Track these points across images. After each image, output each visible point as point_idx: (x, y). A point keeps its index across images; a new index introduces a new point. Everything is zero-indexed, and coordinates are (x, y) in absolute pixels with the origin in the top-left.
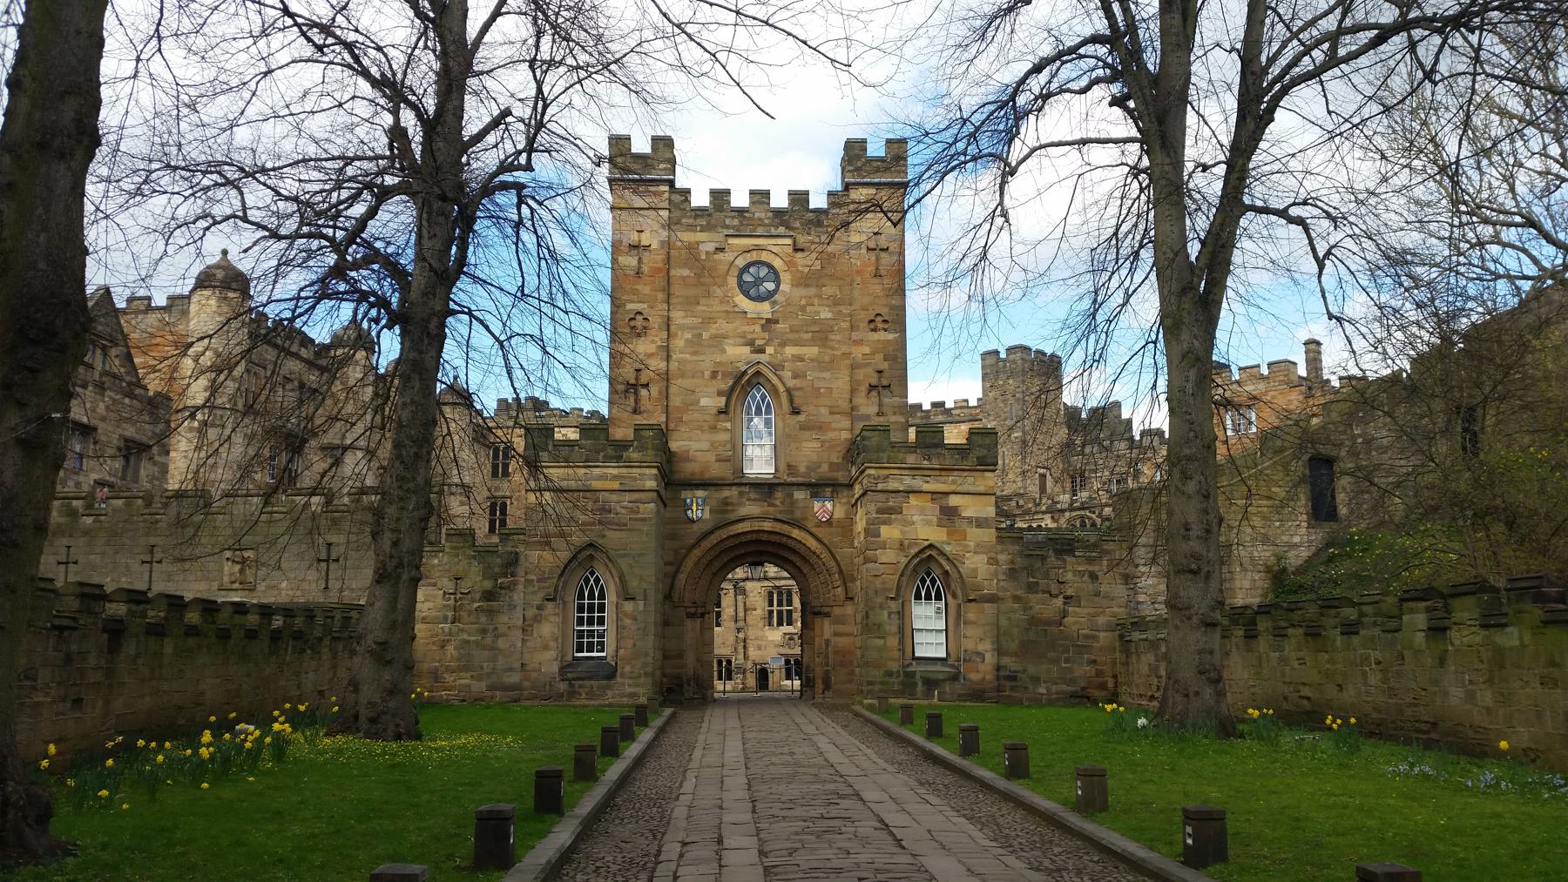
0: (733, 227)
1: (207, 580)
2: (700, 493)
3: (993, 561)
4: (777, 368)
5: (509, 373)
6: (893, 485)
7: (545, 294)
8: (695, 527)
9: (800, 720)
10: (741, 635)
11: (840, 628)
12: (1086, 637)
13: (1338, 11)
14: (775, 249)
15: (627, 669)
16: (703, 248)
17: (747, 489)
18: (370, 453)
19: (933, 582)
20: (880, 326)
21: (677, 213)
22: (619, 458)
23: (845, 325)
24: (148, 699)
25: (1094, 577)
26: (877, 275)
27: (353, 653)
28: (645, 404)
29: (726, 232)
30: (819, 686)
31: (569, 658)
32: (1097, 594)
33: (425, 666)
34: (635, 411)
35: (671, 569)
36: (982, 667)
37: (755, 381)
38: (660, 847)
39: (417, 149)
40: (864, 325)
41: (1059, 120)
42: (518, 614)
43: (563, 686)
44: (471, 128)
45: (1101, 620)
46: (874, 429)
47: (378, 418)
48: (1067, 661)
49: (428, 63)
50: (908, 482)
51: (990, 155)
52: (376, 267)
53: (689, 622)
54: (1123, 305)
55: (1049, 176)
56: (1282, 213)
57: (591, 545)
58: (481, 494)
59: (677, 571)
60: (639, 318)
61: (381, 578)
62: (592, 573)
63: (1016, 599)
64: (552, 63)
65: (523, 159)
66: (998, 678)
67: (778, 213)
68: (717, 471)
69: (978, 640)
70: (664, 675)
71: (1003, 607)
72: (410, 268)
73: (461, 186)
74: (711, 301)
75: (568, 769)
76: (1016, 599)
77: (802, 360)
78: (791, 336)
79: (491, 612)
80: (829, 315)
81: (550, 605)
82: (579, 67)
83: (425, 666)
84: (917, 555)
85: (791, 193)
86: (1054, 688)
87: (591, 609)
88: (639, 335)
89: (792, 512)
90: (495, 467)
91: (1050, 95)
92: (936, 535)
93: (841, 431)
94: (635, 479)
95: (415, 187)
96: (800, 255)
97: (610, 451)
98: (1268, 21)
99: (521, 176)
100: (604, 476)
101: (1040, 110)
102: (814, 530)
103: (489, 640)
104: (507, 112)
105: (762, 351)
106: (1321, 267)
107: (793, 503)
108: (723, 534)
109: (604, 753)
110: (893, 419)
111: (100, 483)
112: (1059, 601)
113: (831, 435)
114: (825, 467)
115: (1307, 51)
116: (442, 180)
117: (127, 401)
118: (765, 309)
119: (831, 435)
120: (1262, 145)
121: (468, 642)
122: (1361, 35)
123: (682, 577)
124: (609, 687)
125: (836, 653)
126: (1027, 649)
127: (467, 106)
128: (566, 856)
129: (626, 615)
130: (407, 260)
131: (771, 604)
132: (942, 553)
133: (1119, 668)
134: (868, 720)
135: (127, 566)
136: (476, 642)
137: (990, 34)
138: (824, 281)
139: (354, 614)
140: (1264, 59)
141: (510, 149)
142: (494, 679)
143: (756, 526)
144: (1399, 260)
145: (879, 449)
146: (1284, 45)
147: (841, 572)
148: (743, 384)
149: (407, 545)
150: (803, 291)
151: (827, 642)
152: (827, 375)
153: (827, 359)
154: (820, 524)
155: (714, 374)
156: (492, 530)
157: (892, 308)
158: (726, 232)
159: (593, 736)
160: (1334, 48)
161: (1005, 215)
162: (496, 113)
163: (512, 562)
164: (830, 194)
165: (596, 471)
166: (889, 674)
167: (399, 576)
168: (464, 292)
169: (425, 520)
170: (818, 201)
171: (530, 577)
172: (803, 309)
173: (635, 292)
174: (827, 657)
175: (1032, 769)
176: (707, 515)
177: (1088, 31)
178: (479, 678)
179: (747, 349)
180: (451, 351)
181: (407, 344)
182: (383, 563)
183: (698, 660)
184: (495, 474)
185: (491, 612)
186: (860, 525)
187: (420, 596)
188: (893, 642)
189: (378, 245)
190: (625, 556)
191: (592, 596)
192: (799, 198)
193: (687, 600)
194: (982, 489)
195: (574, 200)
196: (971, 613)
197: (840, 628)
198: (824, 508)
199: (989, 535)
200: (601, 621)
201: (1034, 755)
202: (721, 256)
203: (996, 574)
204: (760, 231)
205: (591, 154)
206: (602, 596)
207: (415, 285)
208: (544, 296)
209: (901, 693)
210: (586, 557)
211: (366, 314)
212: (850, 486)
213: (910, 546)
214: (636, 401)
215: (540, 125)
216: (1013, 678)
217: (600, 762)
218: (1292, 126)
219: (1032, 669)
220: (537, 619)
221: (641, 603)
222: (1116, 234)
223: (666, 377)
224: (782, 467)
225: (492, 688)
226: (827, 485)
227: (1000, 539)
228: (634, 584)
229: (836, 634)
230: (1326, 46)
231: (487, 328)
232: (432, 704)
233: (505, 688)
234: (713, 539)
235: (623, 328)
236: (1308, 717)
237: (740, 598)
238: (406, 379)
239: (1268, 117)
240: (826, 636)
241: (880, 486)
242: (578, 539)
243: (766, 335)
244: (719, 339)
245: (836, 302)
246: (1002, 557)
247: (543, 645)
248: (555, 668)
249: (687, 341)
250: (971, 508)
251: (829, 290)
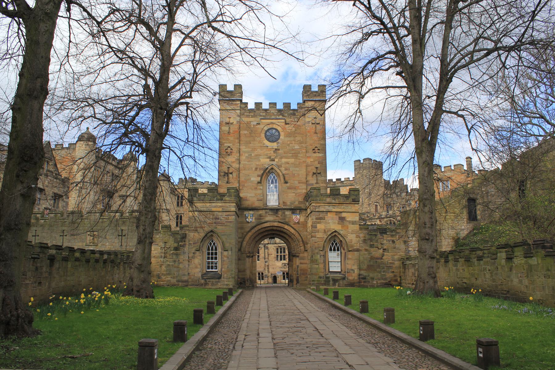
0: (263, 116)
1: (81, 242)
2: (251, 212)
3: (358, 237)
4: (279, 166)
5: (183, 169)
6: (322, 209)
7: (195, 140)
8: (249, 225)
9: (288, 294)
10: (267, 264)
11: (302, 261)
12: (391, 263)
13: (473, 44)
14: (278, 124)
15: (225, 275)
16: (252, 123)
17: (268, 211)
18: (136, 198)
19: (336, 244)
20: (317, 151)
21: (243, 111)
22: (222, 200)
23: (304, 151)
24: (63, 283)
25: (393, 242)
26: (316, 133)
27: (131, 268)
28: (231, 180)
29: (261, 118)
30: (295, 282)
31: (205, 271)
32: (395, 248)
33: (155, 273)
34: (227, 183)
35: (240, 240)
36: (353, 275)
37: (271, 171)
38: (237, 336)
39: (153, 92)
40: (311, 151)
41: (379, 79)
42: (186, 255)
43: (203, 281)
44: (171, 84)
45: (396, 257)
46: (315, 189)
47: (138, 185)
48: (384, 272)
49: (157, 62)
50: (327, 208)
51: (355, 91)
52: (138, 133)
53: (247, 259)
54: (403, 145)
55: (376, 99)
56: (456, 113)
57: (212, 231)
58: (173, 213)
59: (243, 241)
60: (229, 149)
61: (140, 242)
62: (212, 241)
63: (366, 250)
64: (200, 61)
65: (189, 94)
66: (359, 278)
67: (280, 111)
68: (257, 204)
69: (352, 265)
70: (238, 278)
71: (362, 253)
72: (149, 133)
73: (167, 104)
75: (205, 310)
76: (366, 250)
77: (288, 164)
79: (177, 255)
80: (298, 147)
81: (198, 252)
82: (208, 62)
83: (155, 273)
84: (330, 234)
85: (284, 104)
86: (379, 282)
87: (212, 254)
88: (229, 155)
89: (285, 219)
90: (178, 203)
91: (375, 71)
92: (338, 228)
93: (303, 190)
94: (227, 207)
95: (152, 105)
96: (287, 126)
97: (219, 197)
98: (449, 47)
99: (188, 100)
100: (216, 206)
101: (372, 76)
102: (293, 226)
103: (176, 264)
104: (184, 78)
105: (274, 160)
106: (470, 132)
107: (285, 216)
108: (260, 227)
109: (218, 305)
110: (322, 185)
111: (46, 209)
112: (381, 251)
113: (299, 191)
114: (297, 203)
115: (463, 58)
116: (161, 102)
117: (55, 180)
118: (275, 145)
119: (299, 191)
120: (448, 90)
121: (169, 265)
122: (482, 52)
124: (219, 282)
125: (301, 270)
126: (370, 268)
127: (170, 76)
128: (205, 339)
129: (224, 256)
130: (149, 130)
131: (278, 253)
132: (339, 234)
133: (402, 274)
134: (312, 294)
135: (55, 237)
136: (172, 265)
137: (354, 50)
139: (131, 254)
140: (448, 60)
141: (185, 91)
142: (179, 278)
144: (496, 130)
145: (317, 196)
146: (455, 55)
147: (303, 241)
148: (267, 173)
149: (148, 230)
151: (298, 266)
152: (297, 169)
153: (297, 163)
154: (295, 223)
155: (256, 169)
156: (177, 225)
157: (321, 144)
158: (261, 118)
159: (213, 299)
160: (472, 57)
161: (360, 112)
162: (180, 78)
163: (184, 237)
164: (298, 104)
165: (214, 204)
166: (320, 277)
167: (145, 241)
168: (168, 141)
169: (154, 222)
170: (294, 106)
171: (190, 242)
172: (289, 145)
173: (227, 139)
174: (297, 272)
175: (369, 310)
176: (254, 220)
177: (388, 50)
178: (174, 278)
179: (268, 160)
180: (163, 162)
181: (148, 160)
182: (140, 237)
183: (251, 273)
184: (178, 205)
185: (177, 255)
186: (310, 224)
187: (153, 247)
188: (321, 266)
189: (139, 125)
190: (224, 235)
191: (212, 249)
192: (287, 105)
193: (247, 252)
194: (354, 211)
195: (206, 107)
196: (350, 255)
197: (302, 261)
198: (296, 218)
199: (357, 227)
200: (216, 258)
201: (371, 305)
202: (258, 126)
203: (359, 241)
204: (273, 117)
205: (212, 92)
206: (216, 249)
207: (151, 139)
208: (195, 142)
209: (325, 284)
210: (210, 235)
211: (135, 149)
212: (306, 210)
213: (328, 231)
214: (228, 179)
215: (195, 82)
216: (364, 278)
217: (216, 308)
218: (457, 84)
219: (371, 275)
220: (193, 257)
221: (230, 252)
222: (400, 119)
223: (239, 170)
224: (281, 202)
225: (178, 281)
226: (298, 209)
227: (361, 229)
228: (227, 245)
229: (301, 263)
230: (469, 56)
231: (175, 153)
232: (158, 286)
233: (183, 282)
234: (256, 229)
235: (223, 152)
236: (464, 289)
237: (266, 250)
238: (147, 172)
239: (450, 80)
240: (298, 263)
241: (317, 210)
242: (207, 229)
243: (275, 154)
244: (258, 156)
246: (361, 235)
247: (196, 266)
248: (200, 275)
249: (246, 157)
250: (350, 217)
251: (298, 138)
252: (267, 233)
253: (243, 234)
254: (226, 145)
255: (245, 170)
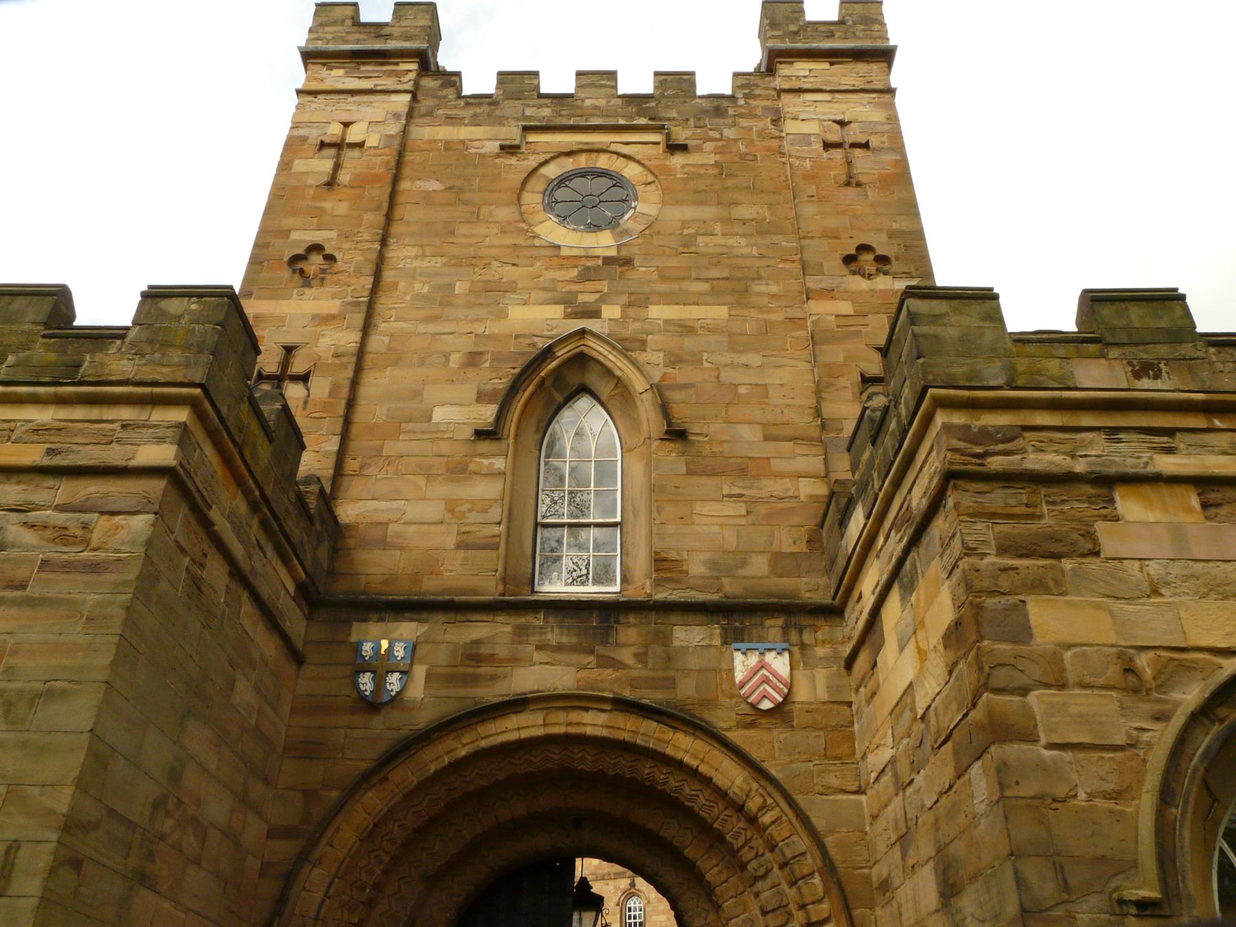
2: (409, 629)
4: (627, 346)
8: (378, 722)
17: (538, 620)
35: (285, 849)
40: (833, 264)
59: (302, 858)
74: (481, 230)
78: (663, 287)
89: (670, 683)
96: (678, 160)
102: (735, 736)
105: (595, 314)
113: (770, 487)
114: (759, 566)
118: (604, 243)
119: (770, 487)
123: (316, 878)
138: (738, 196)
143: (560, 723)
147: (829, 868)
150: (688, 212)
152: (754, 359)
154: (755, 717)
155: (473, 359)
172: (688, 243)
176: (417, 690)
179: (557, 311)
198: (761, 668)
202: (513, 161)
244: (494, 293)
245: (761, 229)
252: (520, 808)
253: (310, 795)
254: (295, 236)
255: (396, 363)
